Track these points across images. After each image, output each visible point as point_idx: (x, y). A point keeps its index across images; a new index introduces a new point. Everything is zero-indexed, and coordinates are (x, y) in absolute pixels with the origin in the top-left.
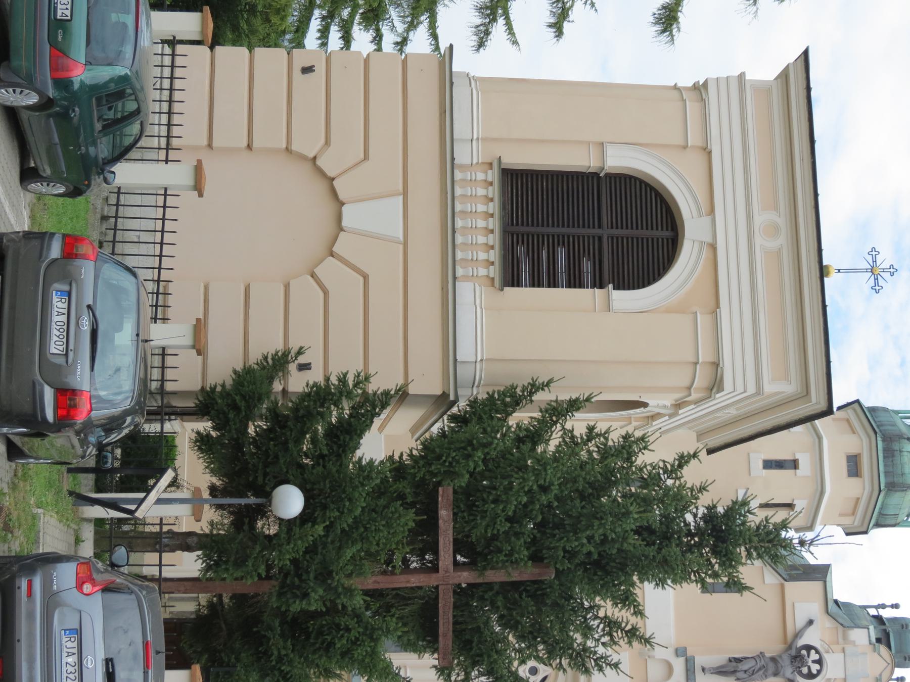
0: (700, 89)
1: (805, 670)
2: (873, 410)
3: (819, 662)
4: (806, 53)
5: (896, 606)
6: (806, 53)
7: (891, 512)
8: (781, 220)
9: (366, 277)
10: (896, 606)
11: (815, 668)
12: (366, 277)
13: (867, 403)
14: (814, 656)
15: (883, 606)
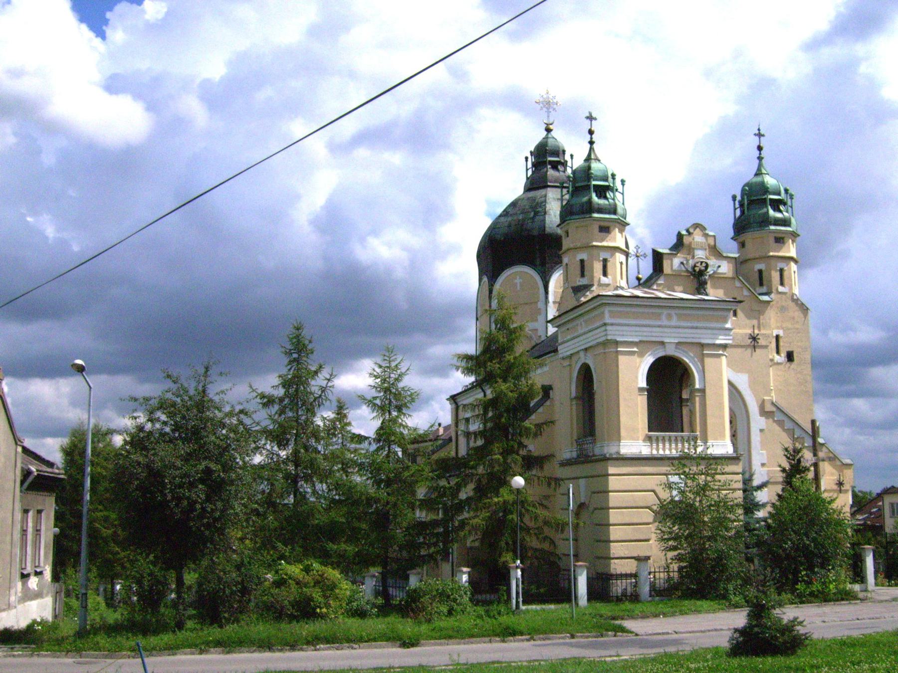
8: (665, 312)
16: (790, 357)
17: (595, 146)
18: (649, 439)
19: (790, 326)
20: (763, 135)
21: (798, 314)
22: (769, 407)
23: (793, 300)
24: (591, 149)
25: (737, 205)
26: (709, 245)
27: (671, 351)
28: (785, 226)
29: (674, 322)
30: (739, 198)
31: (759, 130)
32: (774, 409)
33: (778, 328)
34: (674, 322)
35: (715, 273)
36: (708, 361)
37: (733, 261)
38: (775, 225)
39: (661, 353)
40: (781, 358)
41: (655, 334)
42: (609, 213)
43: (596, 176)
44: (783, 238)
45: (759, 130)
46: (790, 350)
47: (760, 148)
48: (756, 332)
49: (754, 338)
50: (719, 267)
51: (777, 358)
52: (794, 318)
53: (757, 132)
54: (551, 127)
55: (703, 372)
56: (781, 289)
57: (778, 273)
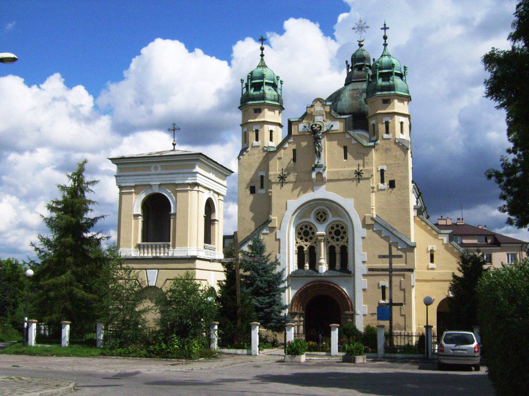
0: (120, 187)
1: (319, 129)
2: (241, 103)
3: (316, 125)
4: (110, 159)
5: (347, 62)
6: (110, 159)
7: (273, 98)
8: (154, 165)
9: (167, 280)
10: (347, 62)
11: (318, 126)
12: (167, 280)
13: (239, 105)
14: (314, 126)
15: (348, 66)
16: (392, 184)
17: (264, 57)
18: (139, 247)
19: (392, 162)
20: (388, 28)
21: (399, 152)
22: (369, 222)
23: (395, 143)
24: (262, 60)
25: (244, 86)
26: (326, 112)
27: (156, 190)
28: (390, 90)
29: (159, 171)
30: (245, 81)
31: (385, 25)
32: (373, 223)
33: (382, 164)
34: (159, 171)
35: (328, 130)
36: (179, 194)
37: (344, 120)
38: (381, 91)
39: (150, 192)
40: (386, 185)
41: (144, 180)
42: (260, 100)
43: (256, 77)
44: (389, 100)
45: (385, 25)
46: (392, 179)
47: (385, 38)
48: (361, 168)
49: (358, 173)
50: (332, 126)
51: (381, 186)
52: (396, 156)
53: (383, 27)
54: (362, 43)
55: (176, 203)
56: (385, 136)
57: (384, 125)
